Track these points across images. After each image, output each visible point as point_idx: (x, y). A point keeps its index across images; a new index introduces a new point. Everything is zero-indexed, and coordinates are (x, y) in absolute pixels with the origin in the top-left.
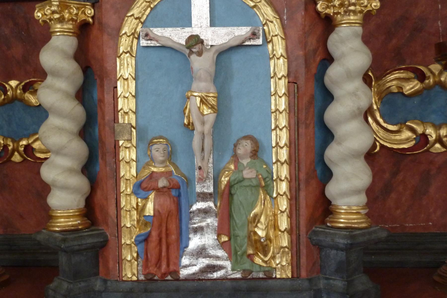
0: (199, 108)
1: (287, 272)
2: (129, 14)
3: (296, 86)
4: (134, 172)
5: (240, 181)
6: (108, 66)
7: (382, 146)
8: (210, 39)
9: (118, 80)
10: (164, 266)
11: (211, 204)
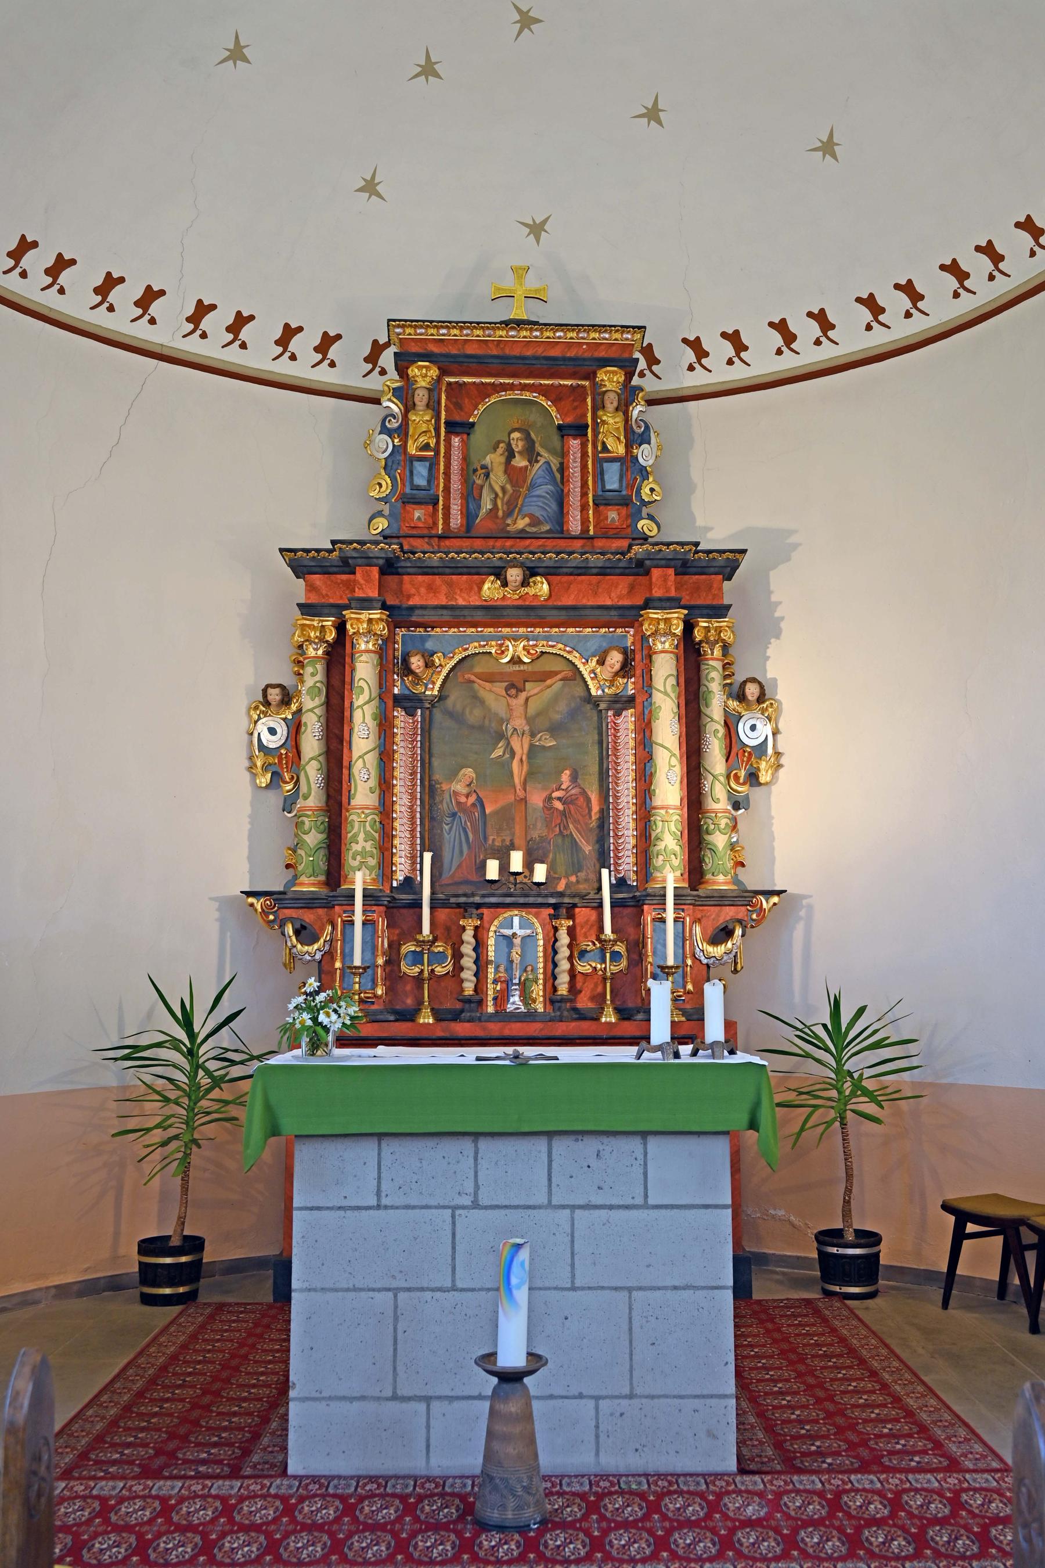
6: (485, 941)
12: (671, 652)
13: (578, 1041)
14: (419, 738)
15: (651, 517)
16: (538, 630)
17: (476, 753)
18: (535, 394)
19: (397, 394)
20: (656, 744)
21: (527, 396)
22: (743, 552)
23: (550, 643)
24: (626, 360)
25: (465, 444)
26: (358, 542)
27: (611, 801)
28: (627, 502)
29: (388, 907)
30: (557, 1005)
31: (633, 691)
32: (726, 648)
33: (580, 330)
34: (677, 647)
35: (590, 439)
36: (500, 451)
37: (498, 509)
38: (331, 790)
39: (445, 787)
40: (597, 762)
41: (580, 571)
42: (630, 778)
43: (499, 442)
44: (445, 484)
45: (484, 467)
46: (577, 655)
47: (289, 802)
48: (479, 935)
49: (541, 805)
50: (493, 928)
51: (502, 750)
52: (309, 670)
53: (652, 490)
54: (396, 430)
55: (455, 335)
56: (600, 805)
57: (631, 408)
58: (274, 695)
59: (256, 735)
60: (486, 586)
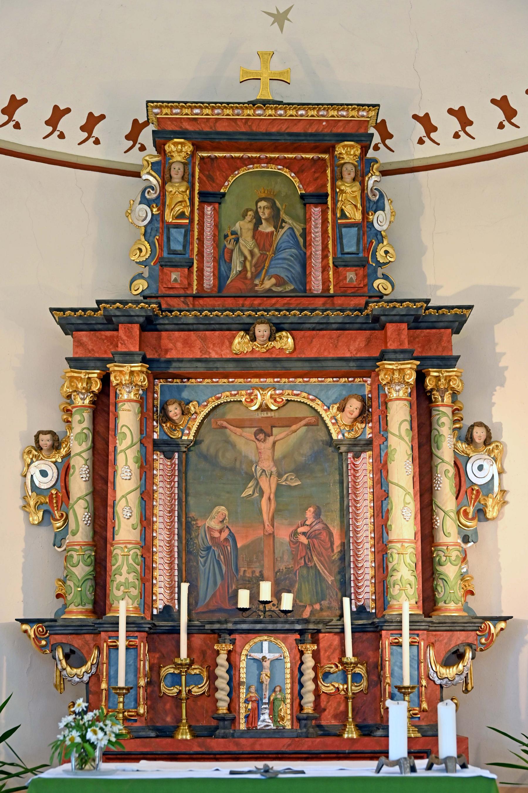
4: (245, 696)
6: (237, 664)
7: (323, 692)
10: (253, 725)
12: (405, 400)
13: (323, 756)
14: (176, 479)
15: (385, 277)
16: (284, 380)
17: (228, 492)
18: (279, 167)
19: (155, 168)
20: (392, 483)
21: (272, 168)
22: (470, 308)
23: (295, 392)
24: (361, 135)
25: (217, 213)
26: (121, 302)
27: (351, 535)
28: (364, 263)
29: (149, 633)
30: (304, 722)
31: (371, 435)
32: (455, 394)
33: (320, 108)
34: (410, 395)
35: (330, 206)
36: (248, 218)
37: (247, 271)
38: (97, 526)
39: (200, 523)
40: (338, 500)
41: (321, 326)
42: (368, 515)
43: (247, 210)
44: (198, 248)
45: (234, 233)
46: (320, 403)
47: (59, 538)
48: (232, 658)
49: (288, 539)
50: (244, 652)
51: (252, 489)
52: (77, 418)
53: (386, 252)
54: (154, 200)
55: (207, 115)
56: (341, 539)
57: (367, 179)
58: (46, 441)
59: (29, 477)
60: (237, 340)
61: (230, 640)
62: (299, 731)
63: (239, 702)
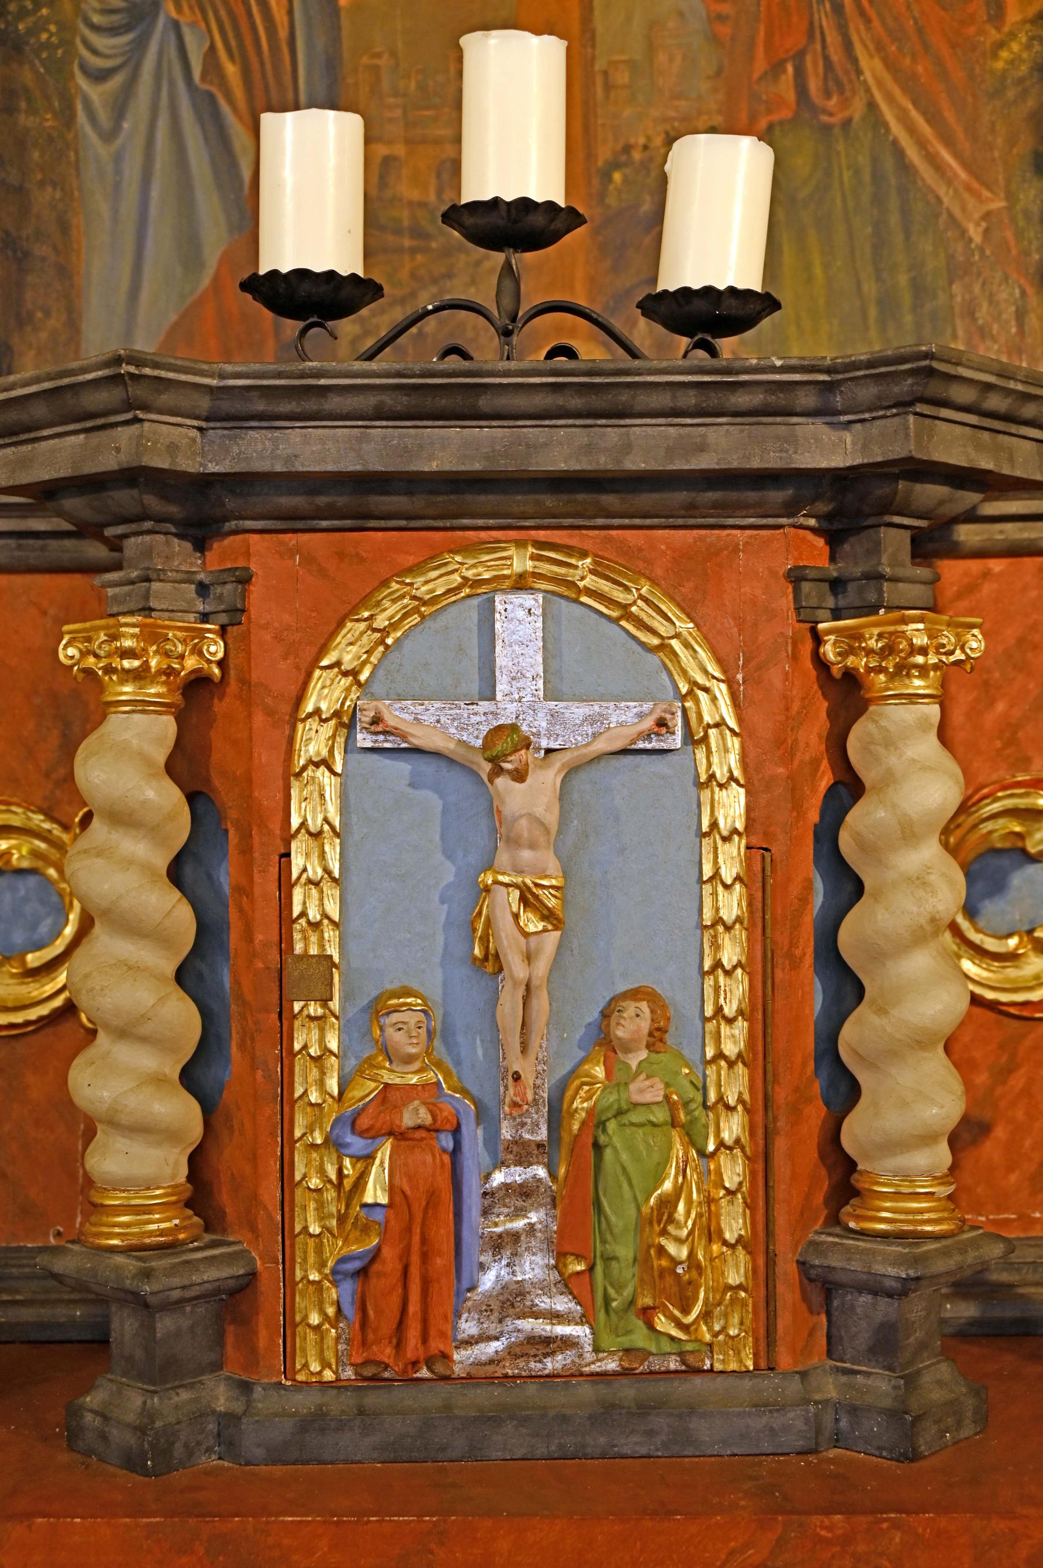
0: (516, 916)
1: (743, 1355)
2: (325, 662)
3: (768, 860)
4: (333, 1084)
5: (620, 1113)
6: (266, 797)
8: (543, 732)
9: (294, 836)
11: (541, 1172)
48: (222, 754)
61: (203, 589)
62: (830, 1388)
63: (288, 1142)
